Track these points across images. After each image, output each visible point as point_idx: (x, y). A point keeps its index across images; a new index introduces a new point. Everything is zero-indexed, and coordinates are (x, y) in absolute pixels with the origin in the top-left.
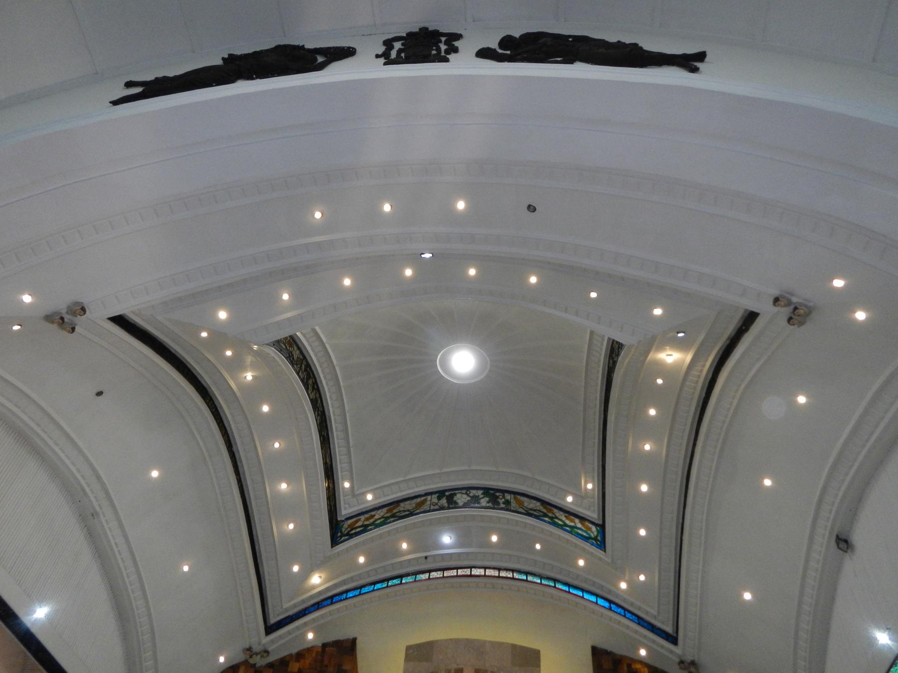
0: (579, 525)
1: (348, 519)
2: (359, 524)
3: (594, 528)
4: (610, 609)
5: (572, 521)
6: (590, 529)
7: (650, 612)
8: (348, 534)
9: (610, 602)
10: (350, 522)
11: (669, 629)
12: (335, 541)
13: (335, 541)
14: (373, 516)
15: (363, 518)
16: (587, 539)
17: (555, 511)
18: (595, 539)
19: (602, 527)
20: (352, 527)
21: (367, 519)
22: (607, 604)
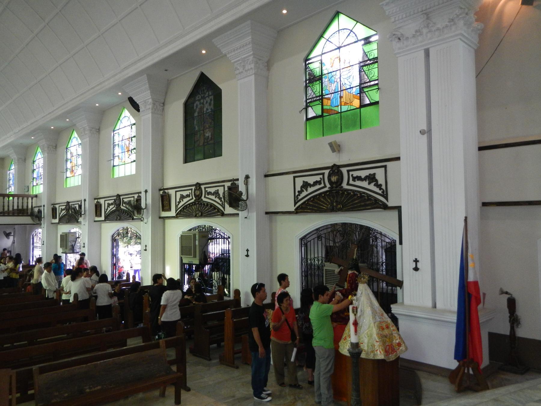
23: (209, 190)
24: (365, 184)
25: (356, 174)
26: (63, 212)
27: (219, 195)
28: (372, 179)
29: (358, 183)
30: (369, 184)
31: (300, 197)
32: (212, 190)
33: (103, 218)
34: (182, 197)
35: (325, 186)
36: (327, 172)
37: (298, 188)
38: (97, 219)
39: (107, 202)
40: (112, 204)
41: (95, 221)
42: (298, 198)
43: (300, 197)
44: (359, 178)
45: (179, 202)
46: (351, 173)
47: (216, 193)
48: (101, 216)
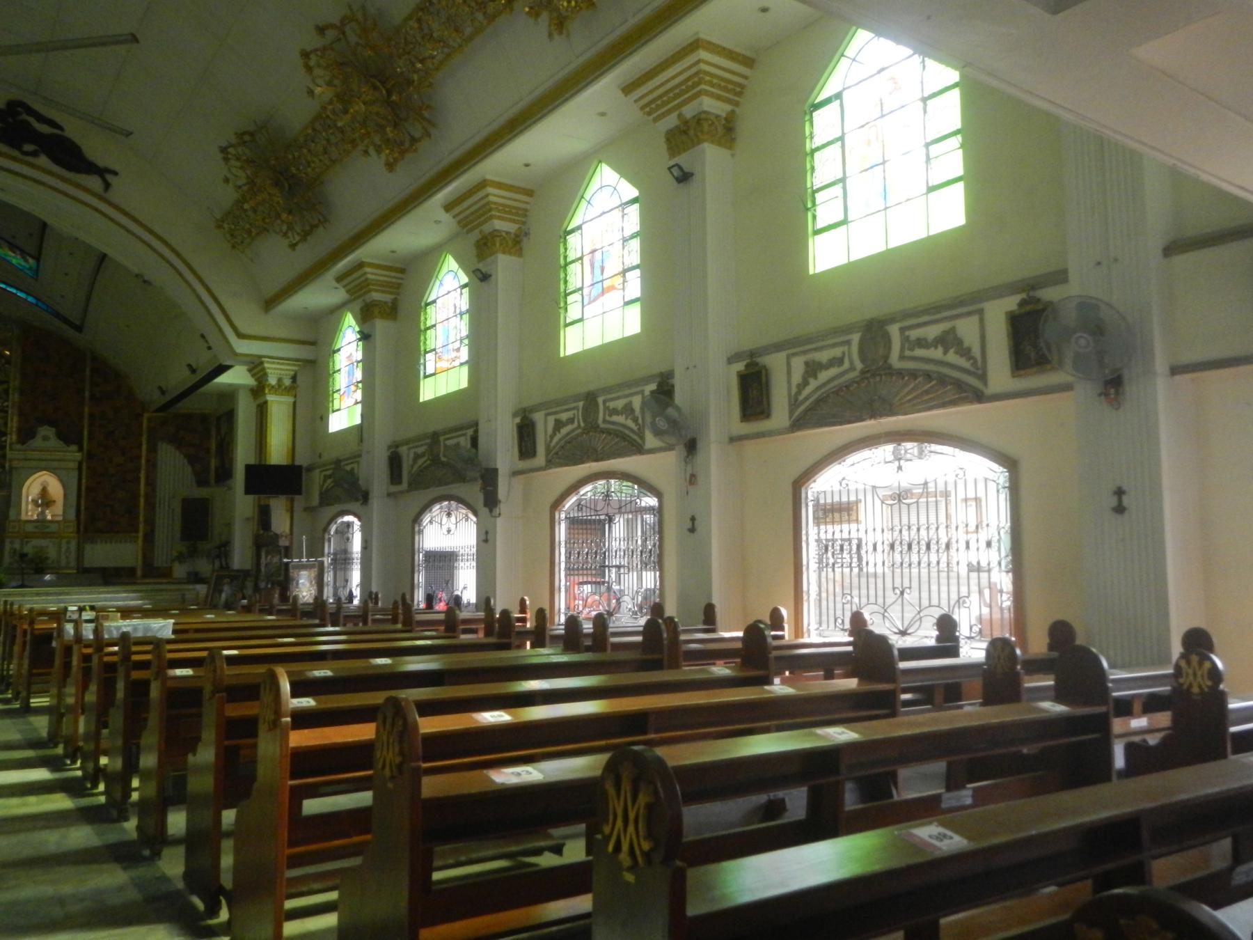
3: (31, 261)
11: (78, 323)
23: (612, 405)
24: (937, 353)
25: (914, 334)
26: (329, 481)
27: (632, 411)
28: (949, 340)
29: (919, 352)
30: (945, 353)
31: (801, 398)
32: (620, 404)
33: (404, 486)
34: (559, 425)
35: (852, 368)
36: (856, 338)
37: (797, 378)
38: (394, 489)
39: (412, 451)
40: (423, 455)
41: (389, 495)
42: (796, 400)
43: (801, 398)
44: (921, 343)
45: (552, 437)
46: (907, 333)
47: (628, 410)
48: (400, 482)
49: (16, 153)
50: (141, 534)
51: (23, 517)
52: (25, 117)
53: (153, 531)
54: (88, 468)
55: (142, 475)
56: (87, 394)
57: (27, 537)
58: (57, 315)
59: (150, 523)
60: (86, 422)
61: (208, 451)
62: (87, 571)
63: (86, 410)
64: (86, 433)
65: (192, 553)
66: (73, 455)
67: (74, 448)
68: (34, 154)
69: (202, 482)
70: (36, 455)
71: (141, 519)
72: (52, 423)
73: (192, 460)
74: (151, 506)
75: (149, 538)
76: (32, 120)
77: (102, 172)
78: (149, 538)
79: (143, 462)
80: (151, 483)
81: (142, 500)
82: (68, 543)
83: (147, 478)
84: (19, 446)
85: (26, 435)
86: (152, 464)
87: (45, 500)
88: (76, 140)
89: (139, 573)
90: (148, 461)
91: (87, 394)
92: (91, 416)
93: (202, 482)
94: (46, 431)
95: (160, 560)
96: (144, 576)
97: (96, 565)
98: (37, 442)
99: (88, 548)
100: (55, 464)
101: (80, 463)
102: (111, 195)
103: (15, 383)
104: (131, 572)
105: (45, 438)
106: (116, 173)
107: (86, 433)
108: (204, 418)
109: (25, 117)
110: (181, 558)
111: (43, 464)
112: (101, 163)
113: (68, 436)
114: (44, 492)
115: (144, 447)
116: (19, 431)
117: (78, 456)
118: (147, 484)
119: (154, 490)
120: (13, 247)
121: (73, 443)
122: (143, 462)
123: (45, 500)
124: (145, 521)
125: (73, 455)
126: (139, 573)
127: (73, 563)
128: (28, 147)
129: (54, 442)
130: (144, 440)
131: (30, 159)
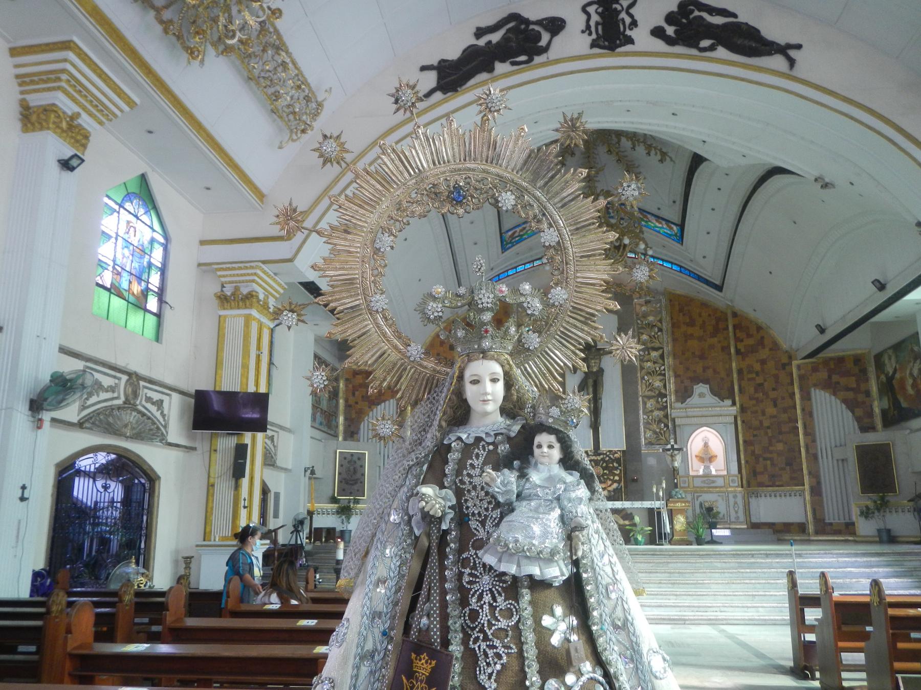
0: (665, 226)
1: (508, 231)
2: (517, 234)
3: (675, 228)
4: (681, 272)
5: (660, 223)
6: (671, 228)
7: (706, 274)
8: (511, 242)
9: (681, 267)
10: (510, 233)
11: (718, 282)
12: (504, 249)
13: (504, 249)
14: (524, 228)
15: (518, 230)
16: (669, 236)
17: (649, 216)
18: (676, 235)
19: (682, 226)
20: (512, 236)
21: (521, 231)
22: (678, 269)
49: (694, 52)
50: (807, 487)
51: (691, 473)
52: (696, 13)
53: (819, 483)
54: (743, 422)
55: (800, 425)
56: (733, 350)
57: (697, 491)
58: (699, 278)
59: (815, 475)
60: (735, 375)
61: (868, 394)
62: (755, 526)
63: (734, 365)
64: (736, 387)
65: (883, 506)
66: (729, 410)
67: (728, 402)
68: (712, 48)
69: (867, 427)
70: (697, 412)
71: (805, 471)
72: (706, 381)
73: (851, 405)
74: (814, 458)
75: (816, 491)
76: (705, 15)
77: (783, 50)
78: (816, 491)
79: (799, 411)
80: (810, 433)
81: (803, 450)
82: (735, 497)
83: (805, 427)
84: (679, 405)
85: (684, 394)
86: (809, 414)
87: (707, 457)
88: (752, 23)
89: (811, 528)
90: (803, 410)
91: (733, 350)
92: (740, 372)
93: (867, 427)
94: (701, 388)
95: (832, 515)
96: (817, 533)
97: (764, 519)
98: (694, 400)
99: (753, 501)
100: (715, 419)
101: (736, 418)
102: (798, 71)
103: (668, 348)
104: (802, 528)
105: (701, 395)
106: (799, 47)
107: (736, 387)
108: (858, 360)
109: (696, 13)
110: (866, 513)
111: (703, 420)
112: (782, 41)
113: (722, 392)
114: (706, 445)
115: (797, 396)
116: (676, 392)
117: (734, 410)
118: (806, 434)
119: (814, 441)
120: (658, 218)
121: (728, 398)
122: (799, 411)
123: (707, 457)
124: (810, 473)
125: (729, 410)
126: (811, 528)
127: (742, 518)
128: (705, 43)
129: (710, 399)
130: (797, 391)
131: (708, 54)
